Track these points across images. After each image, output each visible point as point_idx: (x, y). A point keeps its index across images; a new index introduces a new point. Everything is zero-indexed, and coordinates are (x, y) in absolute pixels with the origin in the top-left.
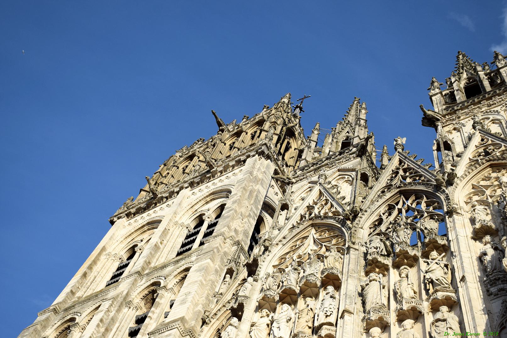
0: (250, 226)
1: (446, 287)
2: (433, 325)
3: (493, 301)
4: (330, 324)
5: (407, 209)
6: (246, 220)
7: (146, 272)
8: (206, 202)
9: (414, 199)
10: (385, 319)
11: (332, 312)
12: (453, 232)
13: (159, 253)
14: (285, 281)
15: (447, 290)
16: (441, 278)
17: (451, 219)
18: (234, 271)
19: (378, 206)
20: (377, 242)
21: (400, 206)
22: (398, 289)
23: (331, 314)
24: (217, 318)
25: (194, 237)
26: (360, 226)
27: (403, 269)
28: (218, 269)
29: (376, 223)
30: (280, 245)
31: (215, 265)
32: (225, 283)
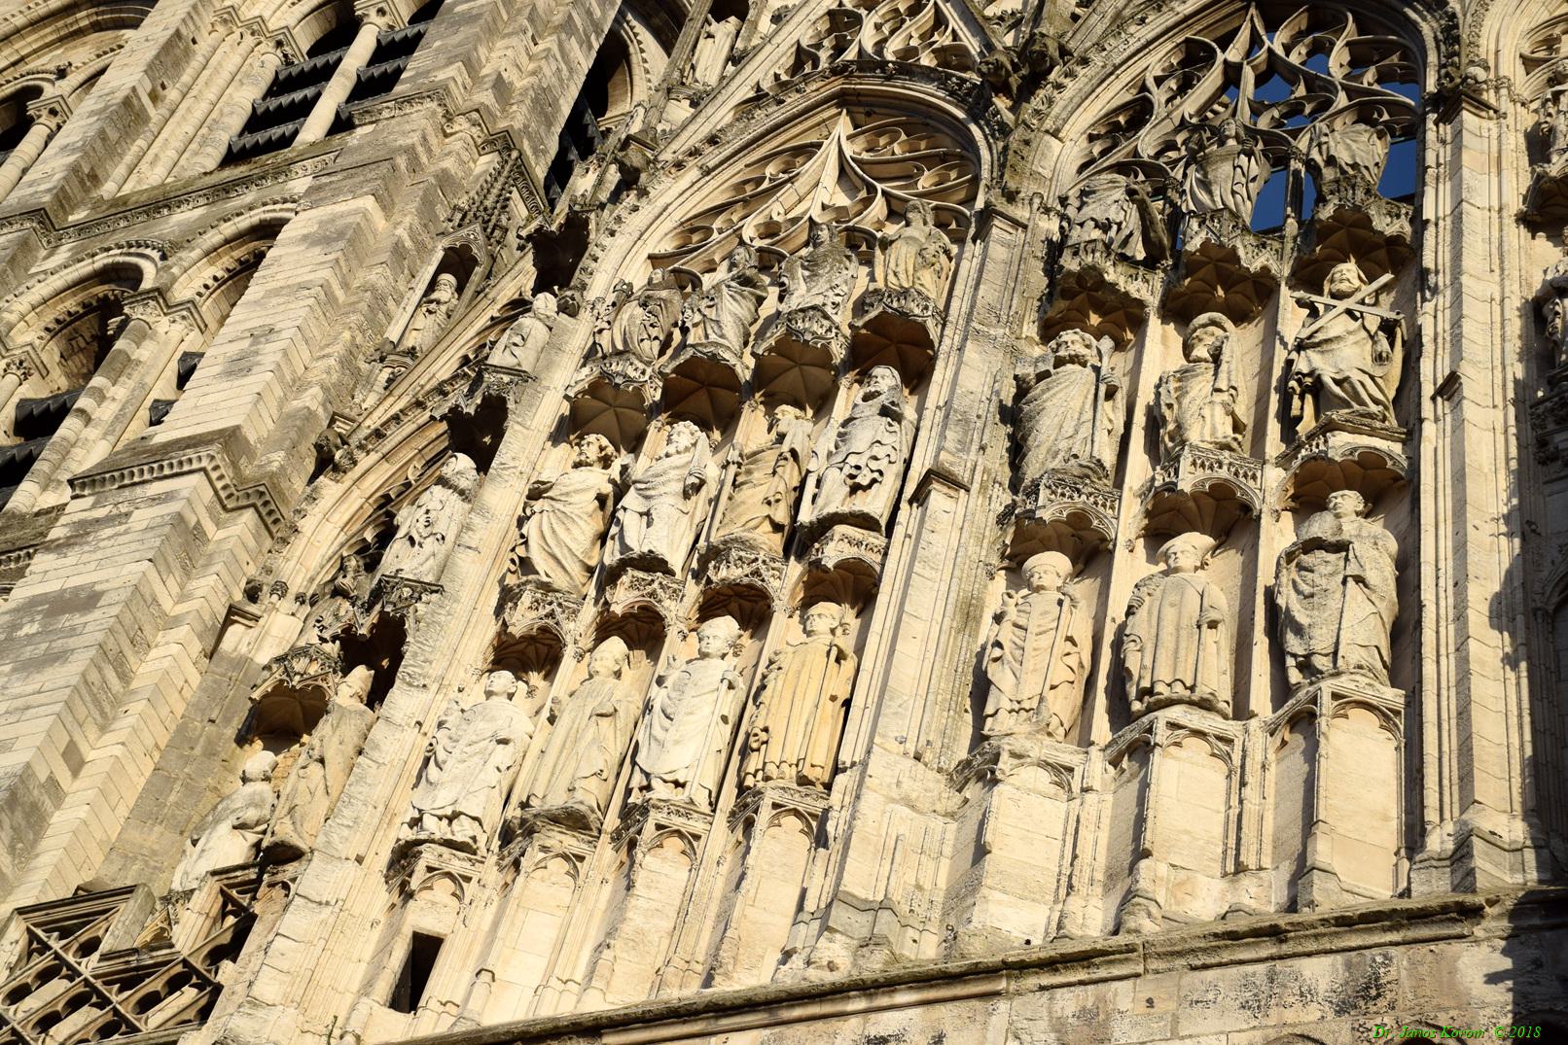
0: (565, 72)
1: (1371, 416)
2: (1289, 562)
3: (1556, 486)
4: (865, 521)
5: (1263, 67)
6: (548, 42)
7: (78, 216)
9: (1303, 28)
10: (1095, 522)
11: (881, 473)
12: (1446, 188)
13: (141, 143)
14: (695, 325)
15: (1373, 429)
16: (1356, 377)
17: (1447, 130)
18: (474, 262)
19: (1138, 45)
20: (1110, 201)
21: (1234, 54)
22: (1170, 406)
23: (874, 481)
24: (385, 450)
25: (309, 92)
26: (1048, 124)
27: (1204, 326)
28: (408, 244)
29: (1122, 119)
30: (692, 174)
31: (396, 225)
32: (433, 306)
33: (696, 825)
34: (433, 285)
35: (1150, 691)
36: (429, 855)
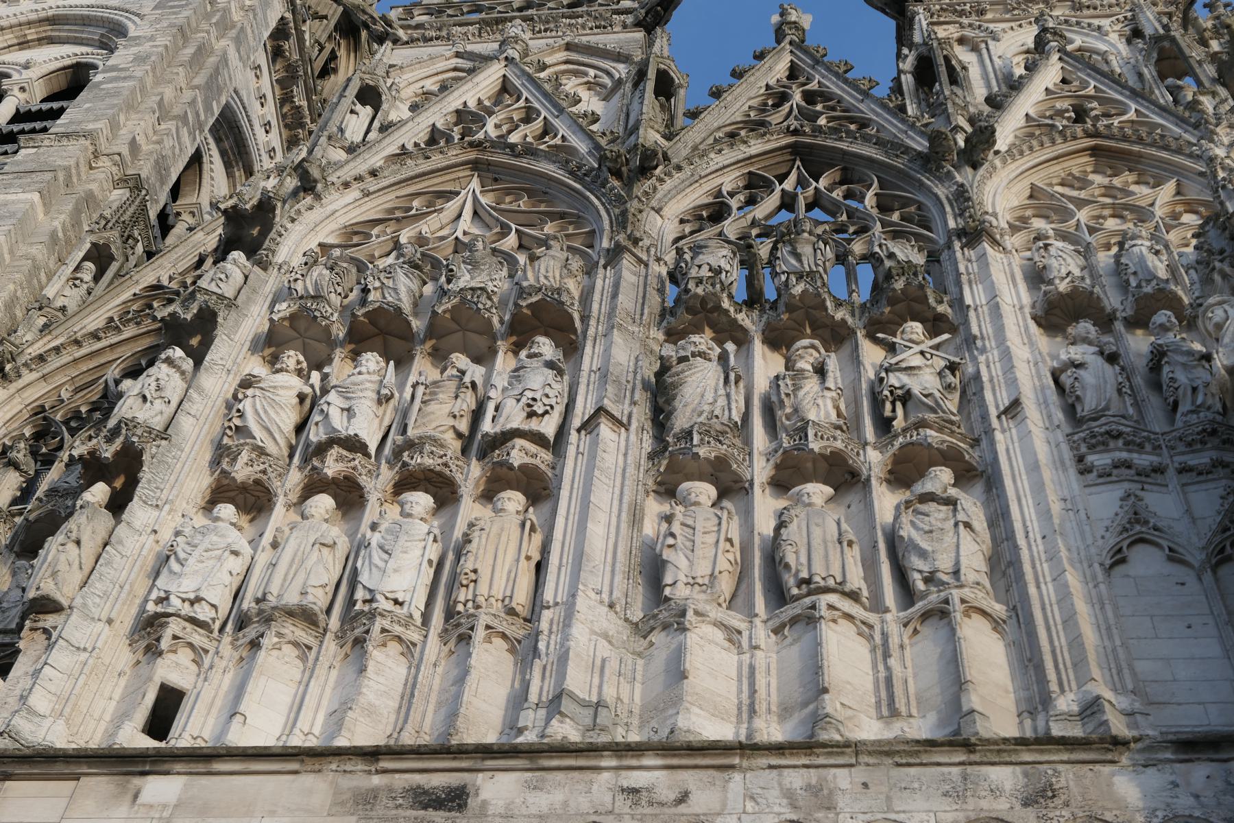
0: (177, 151)
1: (952, 422)
2: (907, 508)
3: (1093, 489)
4: (538, 439)
5: (810, 200)
6: (170, 125)
8: (22, 40)
9: (837, 180)
10: (735, 466)
11: (552, 407)
12: (979, 289)
14: (375, 289)
15: (953, 432)
17: (972, 254)
18: (112, 258)
19: (717, 167)
20: (720, 255)
21: (789, 185)
22: (788, 395)
23: (546, 412)
24: (45, 371)
26: (654, 203)
27: (806, 348)
28: (60, 234)
29: (705, 214)
30: (354, 193)
31: (52, 219)
32: (78, 282)
33: (414, 636)
34: (78, 268)
35: (808, 582)
36: (174, 627)
